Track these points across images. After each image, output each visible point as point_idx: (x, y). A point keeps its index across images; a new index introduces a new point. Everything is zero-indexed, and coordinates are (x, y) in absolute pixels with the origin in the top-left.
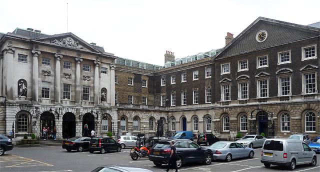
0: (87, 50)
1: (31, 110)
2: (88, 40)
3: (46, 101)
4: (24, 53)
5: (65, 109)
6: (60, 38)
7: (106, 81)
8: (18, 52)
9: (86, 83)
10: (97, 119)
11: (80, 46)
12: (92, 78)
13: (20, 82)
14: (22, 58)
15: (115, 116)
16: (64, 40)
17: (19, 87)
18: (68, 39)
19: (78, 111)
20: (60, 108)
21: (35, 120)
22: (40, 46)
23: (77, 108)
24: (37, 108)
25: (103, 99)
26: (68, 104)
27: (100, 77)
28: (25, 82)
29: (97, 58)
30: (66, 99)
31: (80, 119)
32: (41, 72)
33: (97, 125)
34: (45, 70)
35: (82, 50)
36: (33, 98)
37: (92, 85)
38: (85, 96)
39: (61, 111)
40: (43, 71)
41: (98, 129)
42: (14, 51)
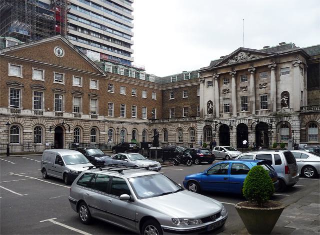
0: (261, 57)
1: (212, 124)
2: (259, 47)
3: (226, 115)
4: (210, 80)
5: (237, 121)
6: (232, 57)
7: (292, 81)
8: (207, 80)
9: (262, 91)
10: (271, 128)
11: (251, 56)
12: (268, 84)
13: (208, 103)
14: (210, 84)
15: (295, 123)
16: (236, 56)
17: (208, 107)
18: (239, 55)
19: (249, 122)
20: (233, 121)
21: (214, 132)
22: (218, 70)
23: (249, 118)
24: (216, 122)
25: (285, 104)
26: (245, 115)
27: (277, 80)
28: (211, 102)
29: (272, 61)
30: (244, 111)
31: (252, 130)
32: (222, 91)
33: (271, 135)
34: (225, 88)
35: (254, 59)
36: (215, 116)
37: (268, 92)
38: (265, 106)
39: (234, 123)
40: (224, 90)
41: (273, 139)
42: (204, 81)
